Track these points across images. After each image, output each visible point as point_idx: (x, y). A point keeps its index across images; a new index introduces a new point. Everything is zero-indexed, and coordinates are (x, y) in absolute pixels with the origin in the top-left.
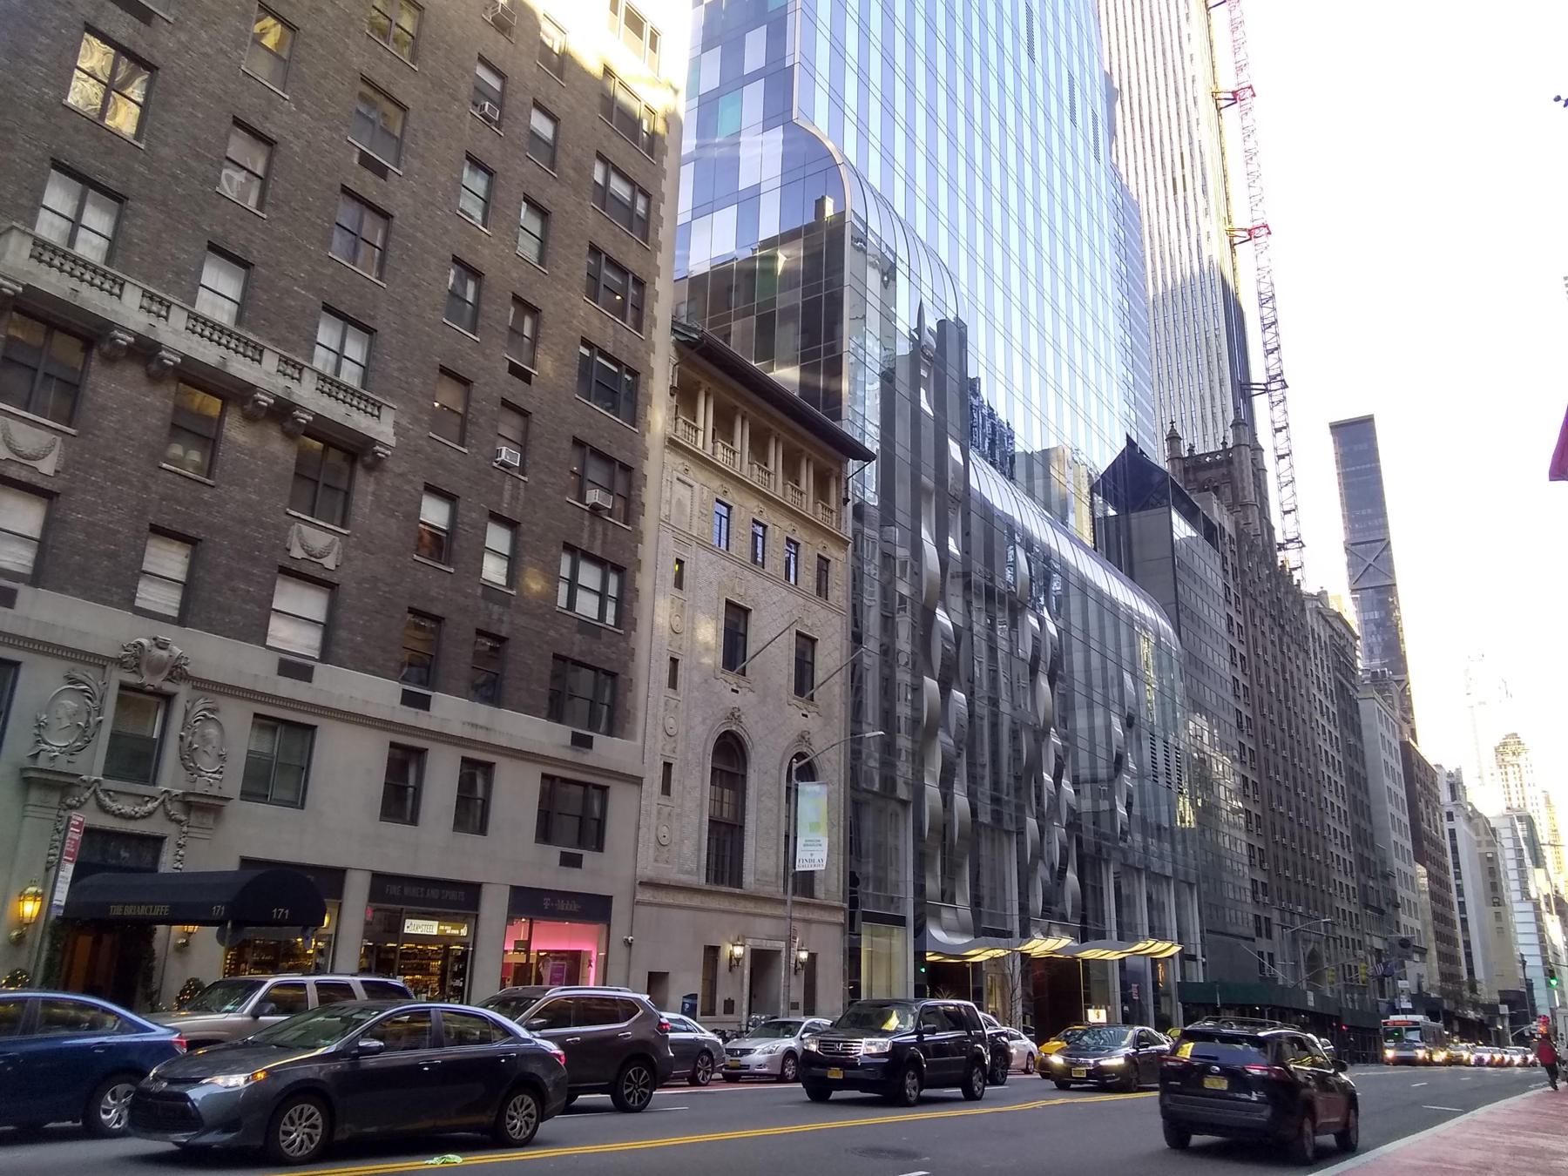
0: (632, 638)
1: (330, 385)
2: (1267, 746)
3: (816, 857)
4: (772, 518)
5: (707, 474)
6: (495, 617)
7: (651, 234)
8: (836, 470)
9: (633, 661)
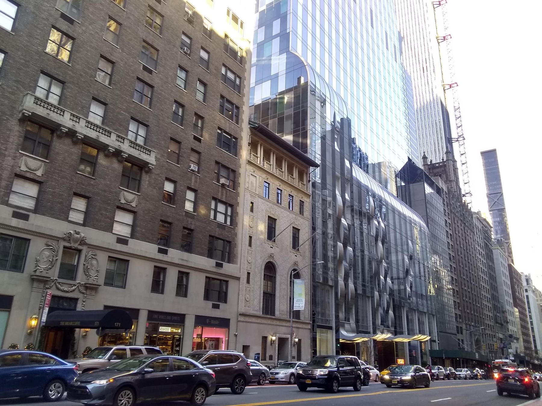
1: (133, 144)
2: (460, 266)
3: (301, 305)
4: (284, 187)
5: (261, 172)
6: (189, 222)
7: (241, 91)
8: (306, 170)
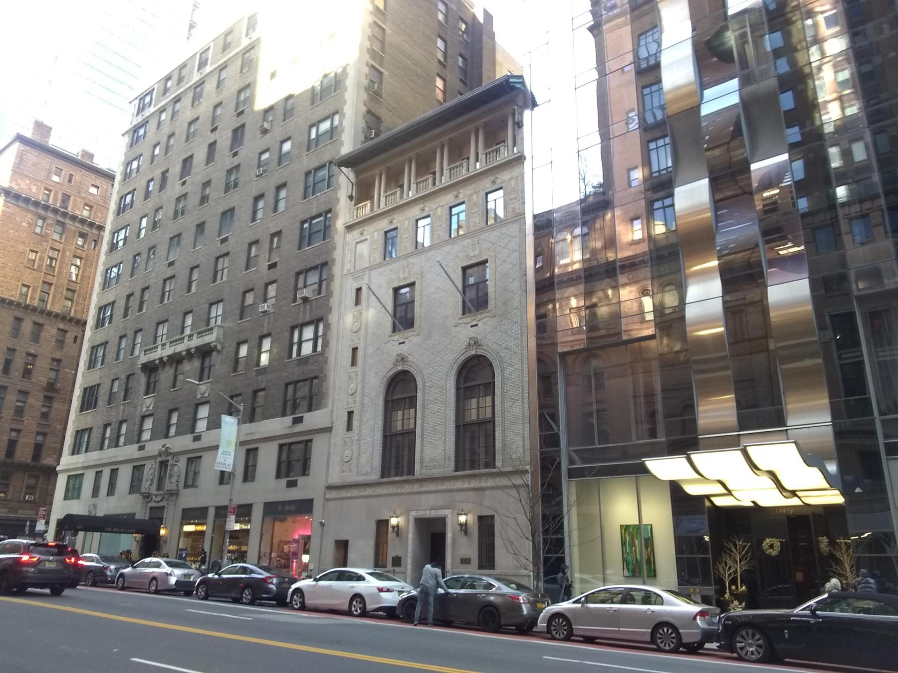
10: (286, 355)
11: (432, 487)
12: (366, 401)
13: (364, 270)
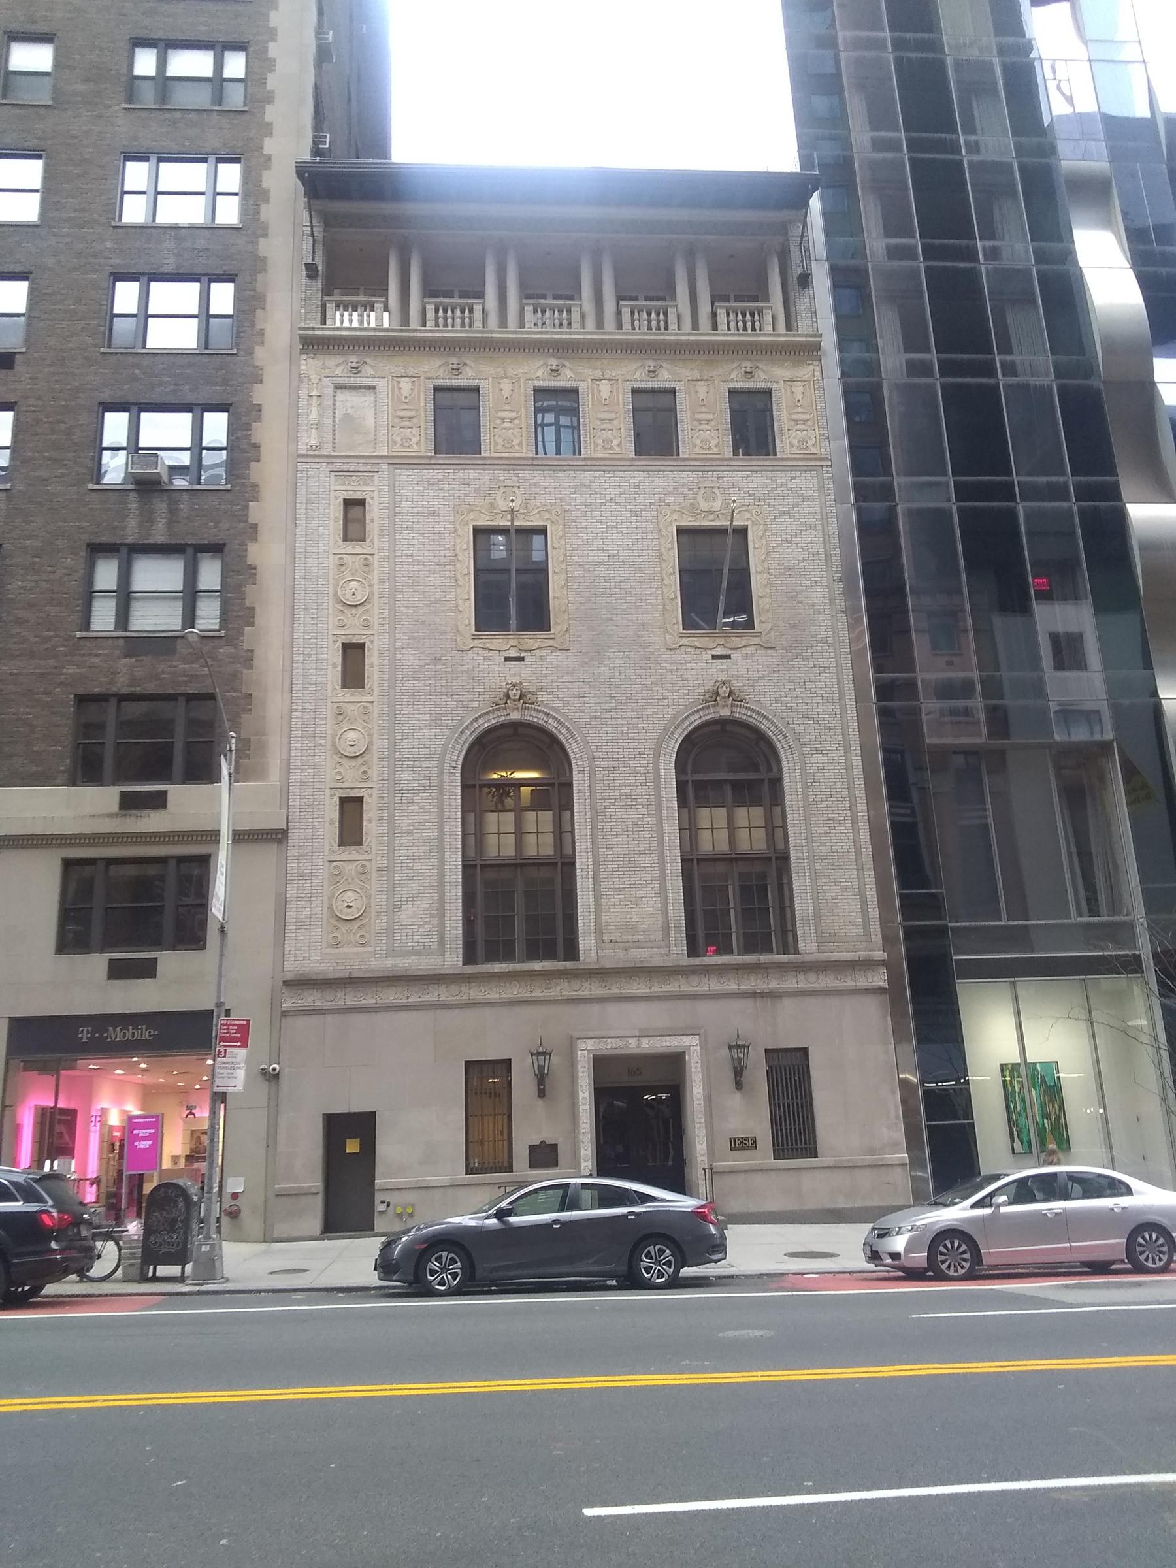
0: (245, 638)
9: (251, 667)
10: (76, 617)
11: (639, 987)
12: (405, 777)
13: (374, 460)
